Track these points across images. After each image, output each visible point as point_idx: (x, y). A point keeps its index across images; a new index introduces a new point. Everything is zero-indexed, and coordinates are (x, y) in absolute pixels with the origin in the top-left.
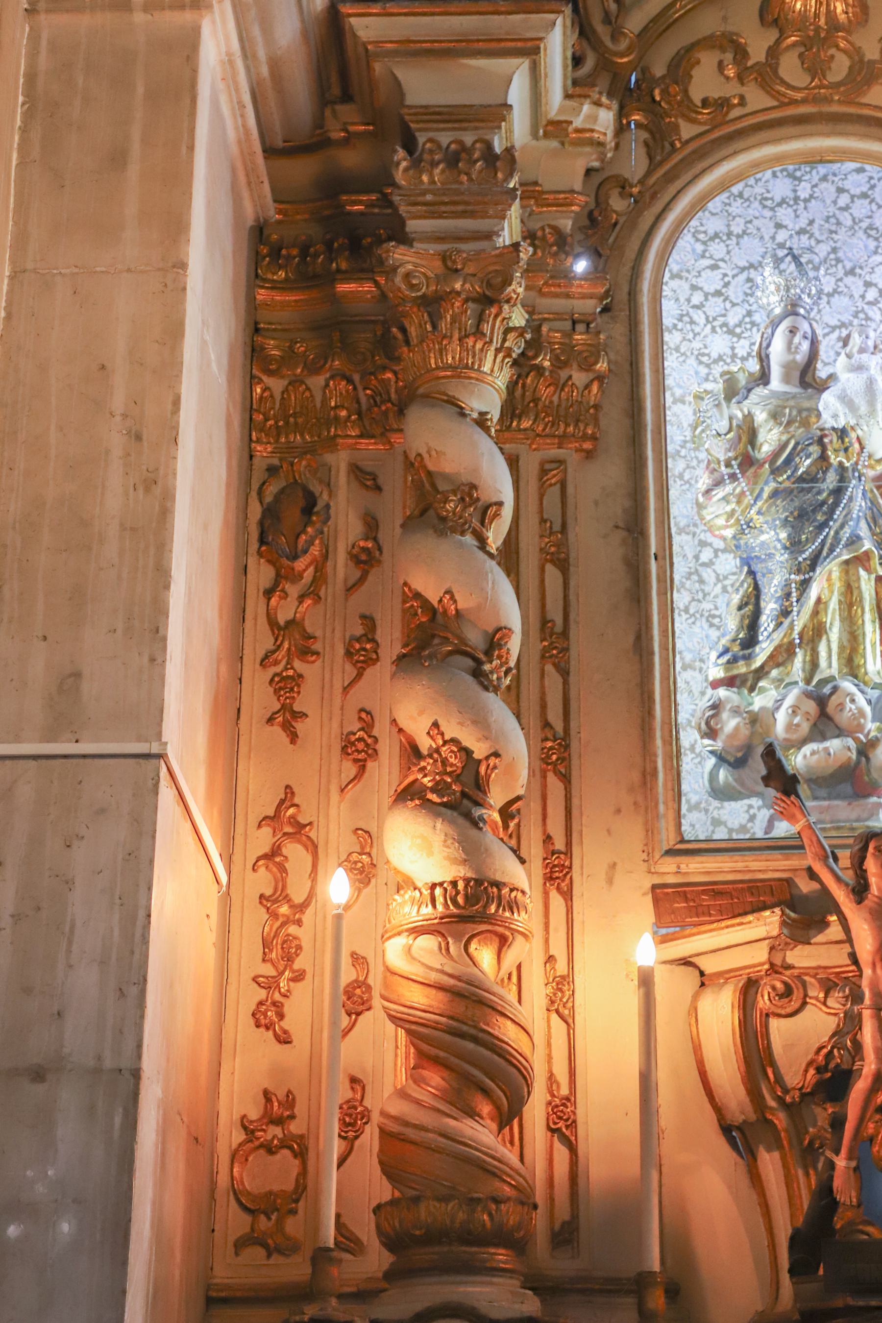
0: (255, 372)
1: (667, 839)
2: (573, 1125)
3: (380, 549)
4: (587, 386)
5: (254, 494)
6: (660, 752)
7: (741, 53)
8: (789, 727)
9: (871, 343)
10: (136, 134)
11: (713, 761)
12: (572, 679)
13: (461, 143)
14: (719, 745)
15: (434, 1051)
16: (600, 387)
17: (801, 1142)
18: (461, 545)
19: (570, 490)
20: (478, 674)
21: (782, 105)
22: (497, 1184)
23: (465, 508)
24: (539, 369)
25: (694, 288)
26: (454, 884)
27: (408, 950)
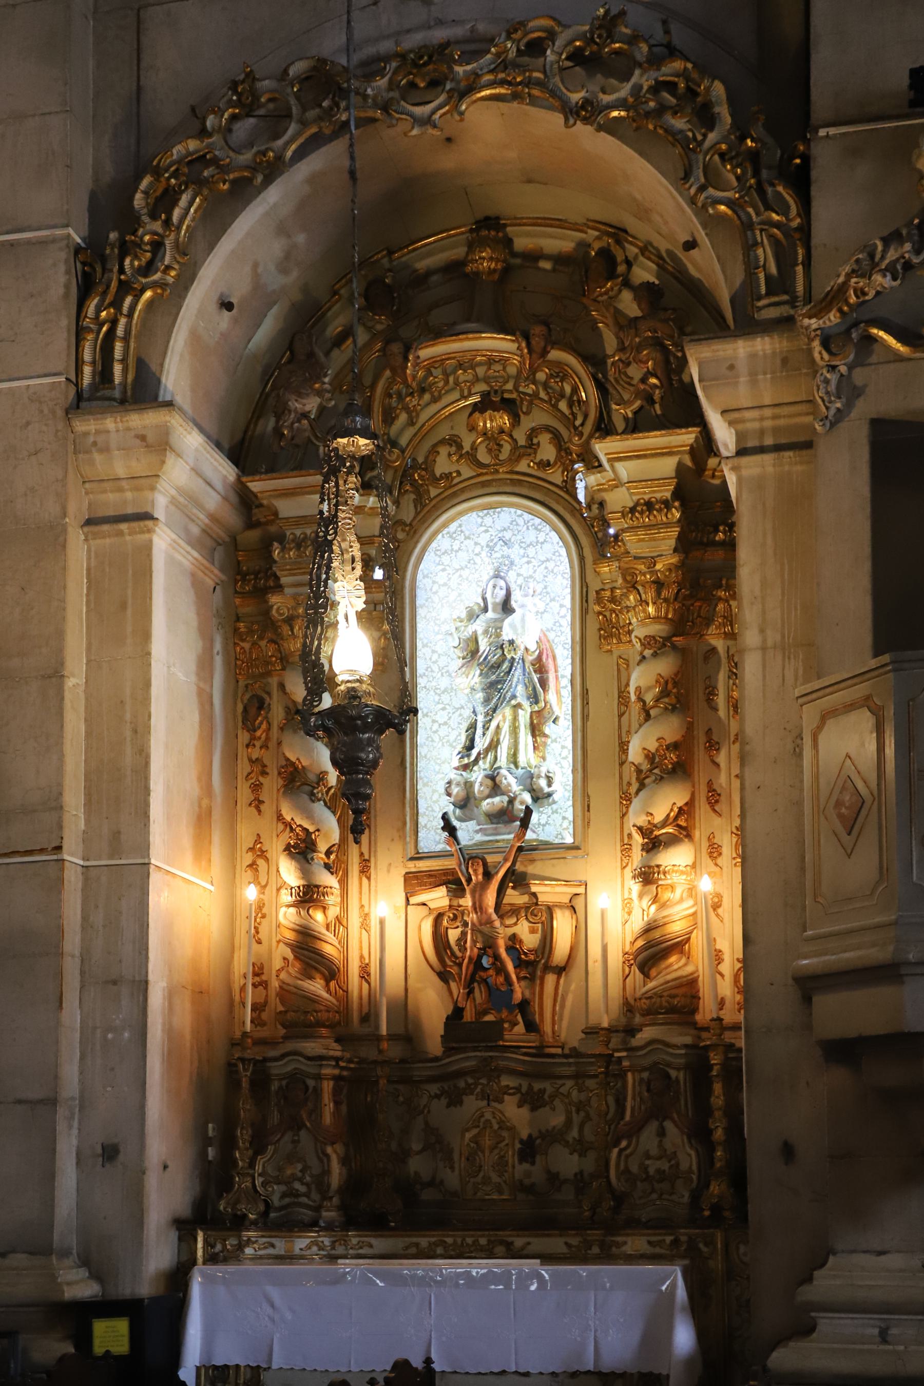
0: (237, 641)
1: (411, 852)
2: (369, 975)
5: (239, 700)
14: (452, 800)
22: (317, 1005)
25: (476, 544)
26: (299, 887)
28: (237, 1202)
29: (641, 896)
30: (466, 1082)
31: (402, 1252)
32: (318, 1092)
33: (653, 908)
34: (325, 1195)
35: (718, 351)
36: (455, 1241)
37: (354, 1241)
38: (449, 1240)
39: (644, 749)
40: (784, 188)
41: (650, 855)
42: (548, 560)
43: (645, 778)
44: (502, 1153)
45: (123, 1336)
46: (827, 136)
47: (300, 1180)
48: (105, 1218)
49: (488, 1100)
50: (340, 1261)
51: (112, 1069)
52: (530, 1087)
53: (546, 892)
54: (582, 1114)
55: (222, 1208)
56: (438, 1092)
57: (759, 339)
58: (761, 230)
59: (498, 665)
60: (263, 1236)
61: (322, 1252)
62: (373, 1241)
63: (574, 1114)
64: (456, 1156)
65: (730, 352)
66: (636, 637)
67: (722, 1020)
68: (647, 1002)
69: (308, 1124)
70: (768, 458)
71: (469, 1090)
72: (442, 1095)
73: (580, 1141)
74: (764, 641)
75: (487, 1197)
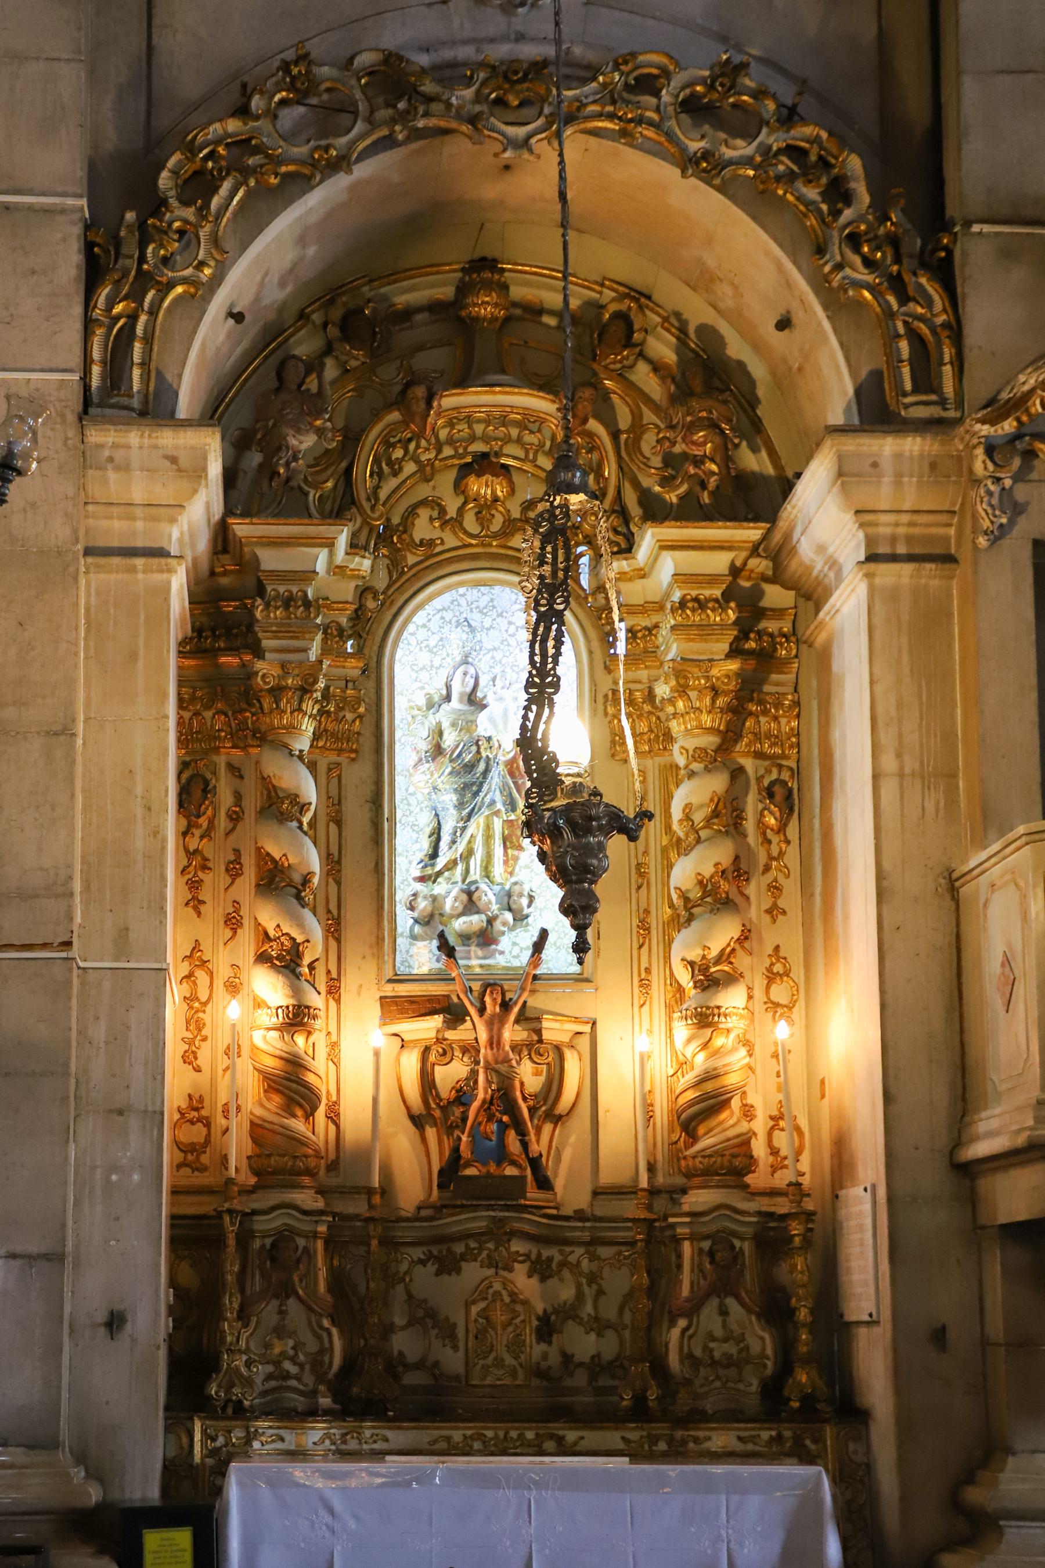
1: (389, 974)
2: (338, 1115)
3: (243, 813)
4: (354, 721)
6: (386, 928)
7: (443, 511)
8: (453, 908)
9: (507, 683)
10: (141, 641)
11: (412, 921)
12: (343, 887)
13: (290, 592)
14: (416, 914)
15: (273, 1085)
16: (361, 722)
17: (446, 1122)
18: (291, 829)
19: (343, 781)
20: (298, 897)
21: (465, 546)
22: (306, 1149)
23: (293, 807)
24: (328, 713)
26: (287, 1007)
27: (265, 1037)
28: (232, 1385)
29: (689, 1041)
30: (467, 1246)
31: (428, 1447)
32: (309, 1254)
33: (700, 1058)
34: (320, 1378)
35: (863, 445)
36: (496, 1434)
37: (368, 1433)
38: (490, 1434)
39: (699, 874)
40: (928, 280)
41: (708, 994)
42: (495, 649)
43: (693, 907)
44: (518, 1332)
45: (185, 1550)
46: (980, 233)
47: (293, 1360)
48: (107, 1403)
49: (497, 1267)
50: (388, 1458)
51: (117, 1219)
52: (539, 1255)
53: (554, 1031)
54: (594, 1287)
55: (213, 1392)
56: (422, 1257)
57: (910, 439)
58: (905, 323)
59: (470, 767)
60: (270, 1427)
61: (333, 1447)
62: (388, 1434)
63: (586, 1289)
64: (461, 1332)
65: (874, 449)
66: (683, 748)
67: (801, 1184)
68: (706, 1160)
69: (301, 1292)
70: (908, 568)
71: (469, 1256)
72: (429, 1260)
73: (597, 1319)
74: (902, 767)
75: (499, 1383)
